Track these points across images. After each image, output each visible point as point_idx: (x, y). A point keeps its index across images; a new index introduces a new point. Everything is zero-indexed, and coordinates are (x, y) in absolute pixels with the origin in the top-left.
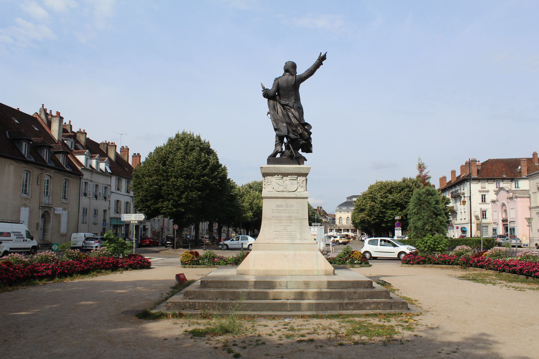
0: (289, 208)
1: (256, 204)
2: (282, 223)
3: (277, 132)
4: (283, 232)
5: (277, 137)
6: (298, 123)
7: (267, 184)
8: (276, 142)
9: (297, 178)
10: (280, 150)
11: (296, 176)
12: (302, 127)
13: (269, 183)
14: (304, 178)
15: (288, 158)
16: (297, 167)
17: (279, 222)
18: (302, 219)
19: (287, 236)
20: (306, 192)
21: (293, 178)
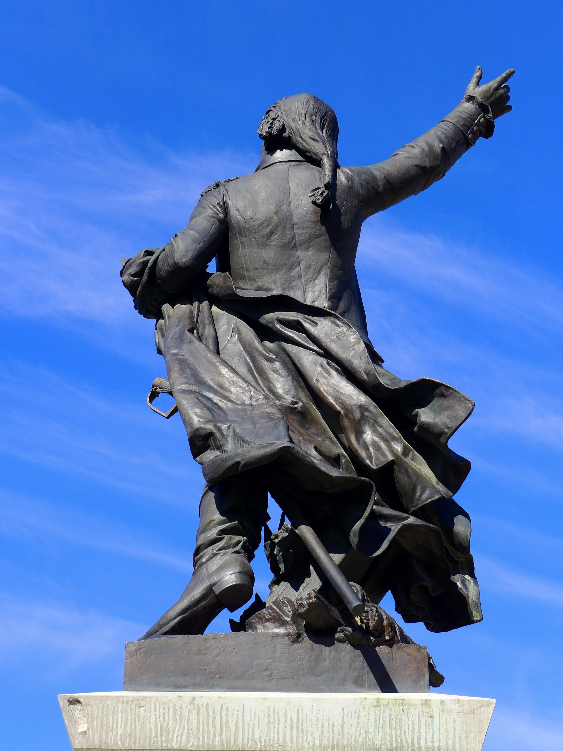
6: (361, 398)
15: (297, 638)
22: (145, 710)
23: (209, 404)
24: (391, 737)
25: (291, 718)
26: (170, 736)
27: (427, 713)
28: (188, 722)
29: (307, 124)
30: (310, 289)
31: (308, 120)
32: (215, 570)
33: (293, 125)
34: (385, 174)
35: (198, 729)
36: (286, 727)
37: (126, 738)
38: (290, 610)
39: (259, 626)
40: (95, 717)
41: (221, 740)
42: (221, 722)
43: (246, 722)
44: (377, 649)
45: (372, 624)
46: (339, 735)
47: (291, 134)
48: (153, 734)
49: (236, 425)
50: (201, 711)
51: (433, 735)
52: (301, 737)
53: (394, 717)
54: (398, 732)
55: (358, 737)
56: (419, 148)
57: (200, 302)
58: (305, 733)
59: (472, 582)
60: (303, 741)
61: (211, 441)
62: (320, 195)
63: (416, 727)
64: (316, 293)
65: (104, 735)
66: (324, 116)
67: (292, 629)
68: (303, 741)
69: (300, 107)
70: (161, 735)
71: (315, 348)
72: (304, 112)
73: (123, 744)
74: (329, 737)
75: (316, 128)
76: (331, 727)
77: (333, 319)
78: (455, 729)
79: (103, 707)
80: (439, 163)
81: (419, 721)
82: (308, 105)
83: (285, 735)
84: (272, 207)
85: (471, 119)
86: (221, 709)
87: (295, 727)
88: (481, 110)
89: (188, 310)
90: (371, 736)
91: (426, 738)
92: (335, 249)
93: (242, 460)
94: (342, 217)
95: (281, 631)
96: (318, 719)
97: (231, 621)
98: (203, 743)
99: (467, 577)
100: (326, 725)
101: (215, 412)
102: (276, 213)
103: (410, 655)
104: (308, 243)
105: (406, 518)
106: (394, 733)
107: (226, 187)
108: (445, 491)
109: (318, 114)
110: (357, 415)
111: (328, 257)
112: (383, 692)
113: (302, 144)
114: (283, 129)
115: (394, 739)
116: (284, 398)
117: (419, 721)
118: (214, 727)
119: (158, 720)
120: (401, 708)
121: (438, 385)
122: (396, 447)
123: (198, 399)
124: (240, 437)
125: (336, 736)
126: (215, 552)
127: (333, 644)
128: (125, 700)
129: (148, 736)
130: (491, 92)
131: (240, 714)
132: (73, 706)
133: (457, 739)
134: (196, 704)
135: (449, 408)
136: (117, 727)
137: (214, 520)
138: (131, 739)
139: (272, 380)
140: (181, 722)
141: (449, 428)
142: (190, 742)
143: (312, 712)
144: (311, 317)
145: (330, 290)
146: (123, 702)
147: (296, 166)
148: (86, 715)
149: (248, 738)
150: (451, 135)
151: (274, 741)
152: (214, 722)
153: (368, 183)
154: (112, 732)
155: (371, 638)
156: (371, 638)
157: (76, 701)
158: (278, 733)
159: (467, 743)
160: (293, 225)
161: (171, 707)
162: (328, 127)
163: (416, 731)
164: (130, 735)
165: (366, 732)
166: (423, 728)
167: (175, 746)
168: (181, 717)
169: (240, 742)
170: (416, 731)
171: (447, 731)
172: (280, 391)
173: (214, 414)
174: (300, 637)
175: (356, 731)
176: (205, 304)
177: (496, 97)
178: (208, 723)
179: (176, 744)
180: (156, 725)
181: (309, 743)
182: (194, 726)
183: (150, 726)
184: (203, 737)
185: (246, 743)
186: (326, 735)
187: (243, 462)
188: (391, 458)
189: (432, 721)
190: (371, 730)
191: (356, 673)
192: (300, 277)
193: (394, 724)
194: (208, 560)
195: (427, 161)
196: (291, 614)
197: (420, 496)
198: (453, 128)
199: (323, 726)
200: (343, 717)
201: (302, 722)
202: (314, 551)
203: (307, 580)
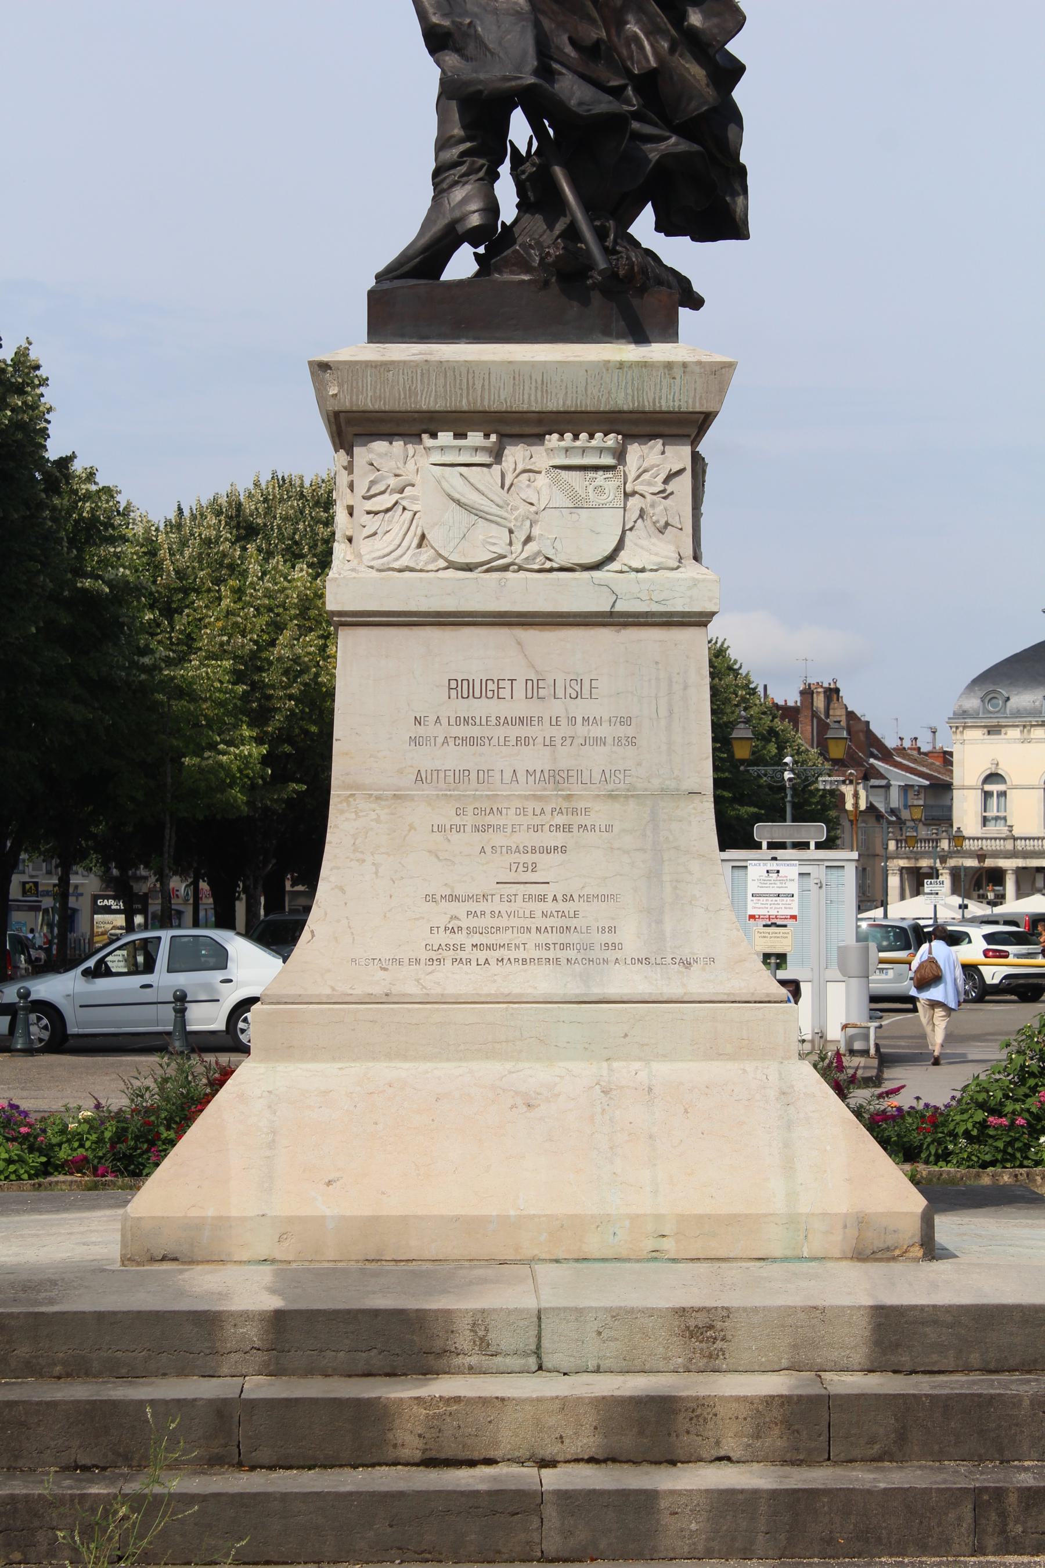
0: (556, 708)
1: (295, 669)
2: (498, 828)
3: (452, 59)
4: (504, 907)
5: (454, 105)
7: (370, 505)
8: (442, 144)
9: (620, 455)
10: (475, 220)
11: (611, 440)
12: (663, 20)
13: (387, 501)
14: (680, 456)
16: (621, 365)
17: (469, 820)
18: (664, 793)
19: (542, 938)
20: (691, 570)
21: (584, 450)
24: (633, 397)
28: (436, 385)
41: (468, 400)
42: (468, 384)
49: (478, 22)
50: (448, 375)
53: (636, 379)
65: (354, 397)
70: (410, 397)
73: (373, 405)
78: (695, 389)
81: (661, 381)
83: (530, 395)
86: (468, 373)
95: (526, 278)
96: (562, 381)
97: (475, 254)
98: (451, 404)
105: (668, 138)
106: (636, 393)
115: (636, 398)
117: (661, 381)
128: (373, 364)
131: (487, 376)
133: (697, 398)
137: (453, 136)
138: (380, 401)
141: (718, 41)
146: (372, 366)
152: (460, 384)
154: (362, 394)
163: (658, 391)
164: (380, 397)
168: (429, 380)
169: (486, 403)
170: (658, 391)
175: (599, 392)
184: (451, 399)
185: (492, 403)
186: (569, 395)
187: (486, 92)
188: (653, 63)
193: (636, 385)
196: (537, 259)
199: (566, 387)
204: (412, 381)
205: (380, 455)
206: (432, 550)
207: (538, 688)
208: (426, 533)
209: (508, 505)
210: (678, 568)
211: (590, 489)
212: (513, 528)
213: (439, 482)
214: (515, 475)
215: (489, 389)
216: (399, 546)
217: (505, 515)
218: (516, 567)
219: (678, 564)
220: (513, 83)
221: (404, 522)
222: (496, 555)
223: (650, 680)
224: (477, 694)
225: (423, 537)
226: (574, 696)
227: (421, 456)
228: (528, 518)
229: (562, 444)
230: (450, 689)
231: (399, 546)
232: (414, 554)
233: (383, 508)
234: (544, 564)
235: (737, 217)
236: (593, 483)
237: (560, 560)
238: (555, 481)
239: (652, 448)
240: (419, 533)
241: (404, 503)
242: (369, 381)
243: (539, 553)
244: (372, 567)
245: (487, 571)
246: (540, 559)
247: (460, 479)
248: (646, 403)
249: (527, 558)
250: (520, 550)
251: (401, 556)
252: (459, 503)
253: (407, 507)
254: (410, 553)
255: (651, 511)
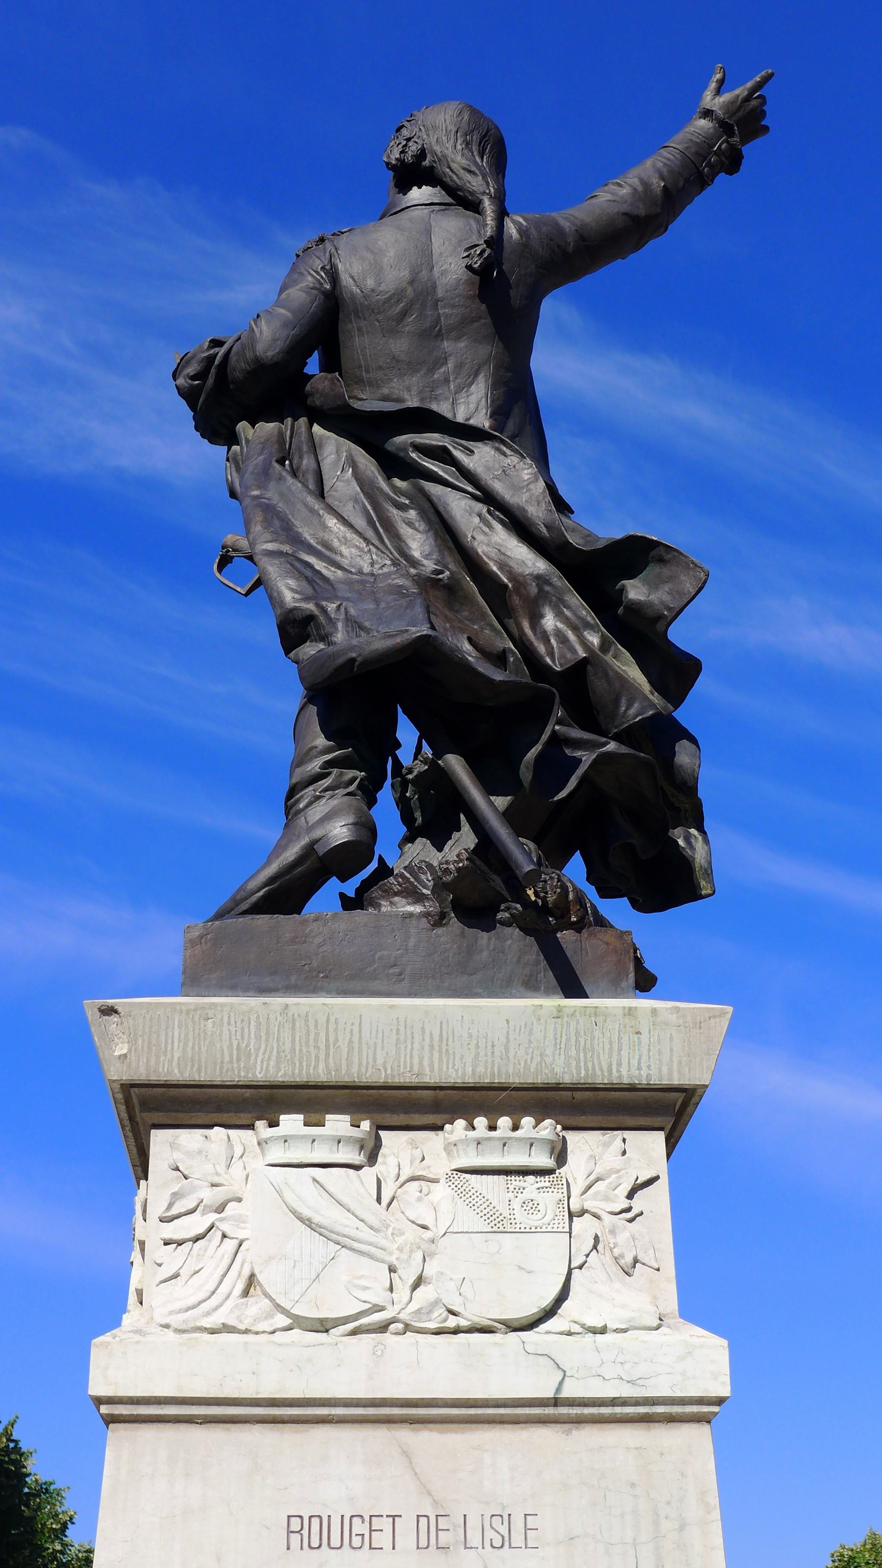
7: (171, 1231)
9: (561, 1158)
11: (548, 1128)
13: (196, 1224)
15: (439, 920)
22: (214, 1023)
23: (308, 573)
24: (578, 1062)
25: (431, 1034)
26: (252, 1062)
27: (632, 1027)
28: (278, 1041)
29: (459, 147)
30: (462, 400)
31: (459, 142)
32: (317, 821)
33: (437, 149)
34: (577, 226)
35: (293, 1050)
36: (423, 1048)
37: (186, 1065)
38: (430, 878)
39: (383, 903)
40: (140, 1033)
41: (327, 1066)
42: (327, 1040)
43: (364, 1040)
44: (559, 935)
45: (551, 898)
46: (502, 1059)
47: (435, 162)
48: (227, 1059)
49: (350, 604)
50: (298, 1024)
51: (640, 1059)
52: (445, 1062)
53: (582, 1033)
54: (589, 1055)
55: (529, 1061)
56: (628, 188)
57: (295, 419)
58: (452, 1057)
59: (700, 838)
60: (448, 1068)
61: (312, 627)
62: (479, 255)
63: (616, 1046)
64: (472, 406)
66: (485, 136)
67: (432, 907)
68: (448, 1068)
69: (448, 122)
70: (238, 1060)
71: (470, 489)
72: (454, 130)
73: (181, 1073)
74: (486, 1061)
75: (473, 153)
76: (490, 1047)
77: (497, 445)
78: (671, 1050)
79: (151, 1019)
80: (659, 210)
81: (620, 1038)
82: (460, 119)
83: (421, 1059)
84: (405, 274)
85: (708, 144)
86: (328, 1021)
87: (436, 1047)
88: (723, 131)
89: (277, 430)
90: (548, 1060)
91: (629, 1063)
92: (500, 339)
93: (360, 655)
94: (511, 291)
95: (417, 909)
96: (470, 1036)
97: (342, 896)
98: (301, 1070)
99: (693, 831)
100: (482, 1044)
101: (318, 584)
102: (412, 282)
103: (607, 944)
104: (459, 329)
105: (605, 744)
106: (582, 1055)
107: (335, 243)
108: (663, 705)
109: (475, 132)
110: (533, 589)
111: (491, 350)
112: (566, 998)
113: (450, 177)
114: (422, 154)
115: (582, 1064)
116: (423, 565)
118: (317, 1047)
119: (233, 1037)
120: (593, 1019)
121: (656, 544)
122: (590, 638)
123: (291, 565)
124: (356, 622)
125: (497, 1060)
126: (318, 794)
127: (494, 928)
128: (184, 1008)
129: (219, 1061)
130: (739, 104)
131: (356, 1028)
132: (107, 1017)
133: (675, 1065)
134: (290, 1015)
135: (671, 579)
136: (173, 1048)
137: (317, 747)
138: (193, 1066)
139: (404, 537)
140: (267, 1040)
141: (669, 609)
142: (281, 1070)
143: (462, 1027)
144: (463, 442)
145: (492, 401)
146: (181, 1012)
147: (441, 212)
148: (127, 1031)
149: (368, 1063)
150: (677, 169)
151: (405, 1068)
152: (316, 1040)
153: (551, 240)
154: (165, 1055)
155: (551, 919)
156: (551, 919)
157: (110, 1011)
158: (411, 1057)
159: (689, 1070)
160: (437, 301)
161: (253, 1018)
162: (490, 152)
163: (615, 1053)
164: (192, 1059)
165: (541, 1055)
166: (625, 1048)
167: (259, 1076)
168: (268, 1034)
169: (355, 1070)
170: (615, 1053)
171: (660, 1053)
172: (416, 554)
173: (317, 587)
174: (445, 918)
176: (303, 421)
177: (746, 112)
178: (307, 1042)
179: (260, 1073)
180: (231, 1044)
181: (457, 1071)
182: (288, 1046)
183: (221, 1046)
184: (301, 1063)
185: (363, 1070)
187: (359, 659)
188: (582, 654)
189: (639, 1038)
190: (549, 1052)
191: (527, 971)
192: (447, 381)
193: (582, 1043)
194: (307, 806)
195: (641, 206)
196: (431, 884)
197: (626, 711)
198: (680, 157)
199: (477, 1046)
200: (508, 1032)
201: (447, 1040)
202: (468, 793)
203: (456, 835)
204: (242, 1033)
205: (189, 1154)
206: (267, 1301)
207: (437, 1530)
208: (256, 1272)
209: (388, 1226)
210: (657, 1328)
211: (516, 1204)
212: (395, 1262)
213: (279, 1193)
214: (398, 1183)
215: (360, 1049)
216: (213, 1293)
217: (383, 1242)
218: (400, 1326)
219: (659, 1322)
220: (398, 640)
221: (223, 1256)
222: (368, 1306)
223: (622, 1515)
224: (335, 1541)
225: (252, 1280)
226: (497, 1543)
227: (254, 1157)
228: (419, 1248)
229: (472, 1134)
230: (290, 1532)
231: (213, 1293)
232: (236, 1306)
233: (192, 1234)
234: (445, 1320)
235: (697, 865)
236: (519, 1195)
237: (472, 1314)
238: (461, 1192)
239: (607, 1145)
240: (246, 1273)
241: (225, 1227)
242: (176, 1034)
243: (437, 1302)
244: (167, 1326)
245: (354, 1333)
246: (441, 1312)
247: (313, 1188)
248: (598, 1072)
249: (418, 1311)
250: (407, 1298)
251: (216, 1309)
252: (308, 1223)
253: (229, 1233)
254: (230, 1303)
255: (612, 1241)
